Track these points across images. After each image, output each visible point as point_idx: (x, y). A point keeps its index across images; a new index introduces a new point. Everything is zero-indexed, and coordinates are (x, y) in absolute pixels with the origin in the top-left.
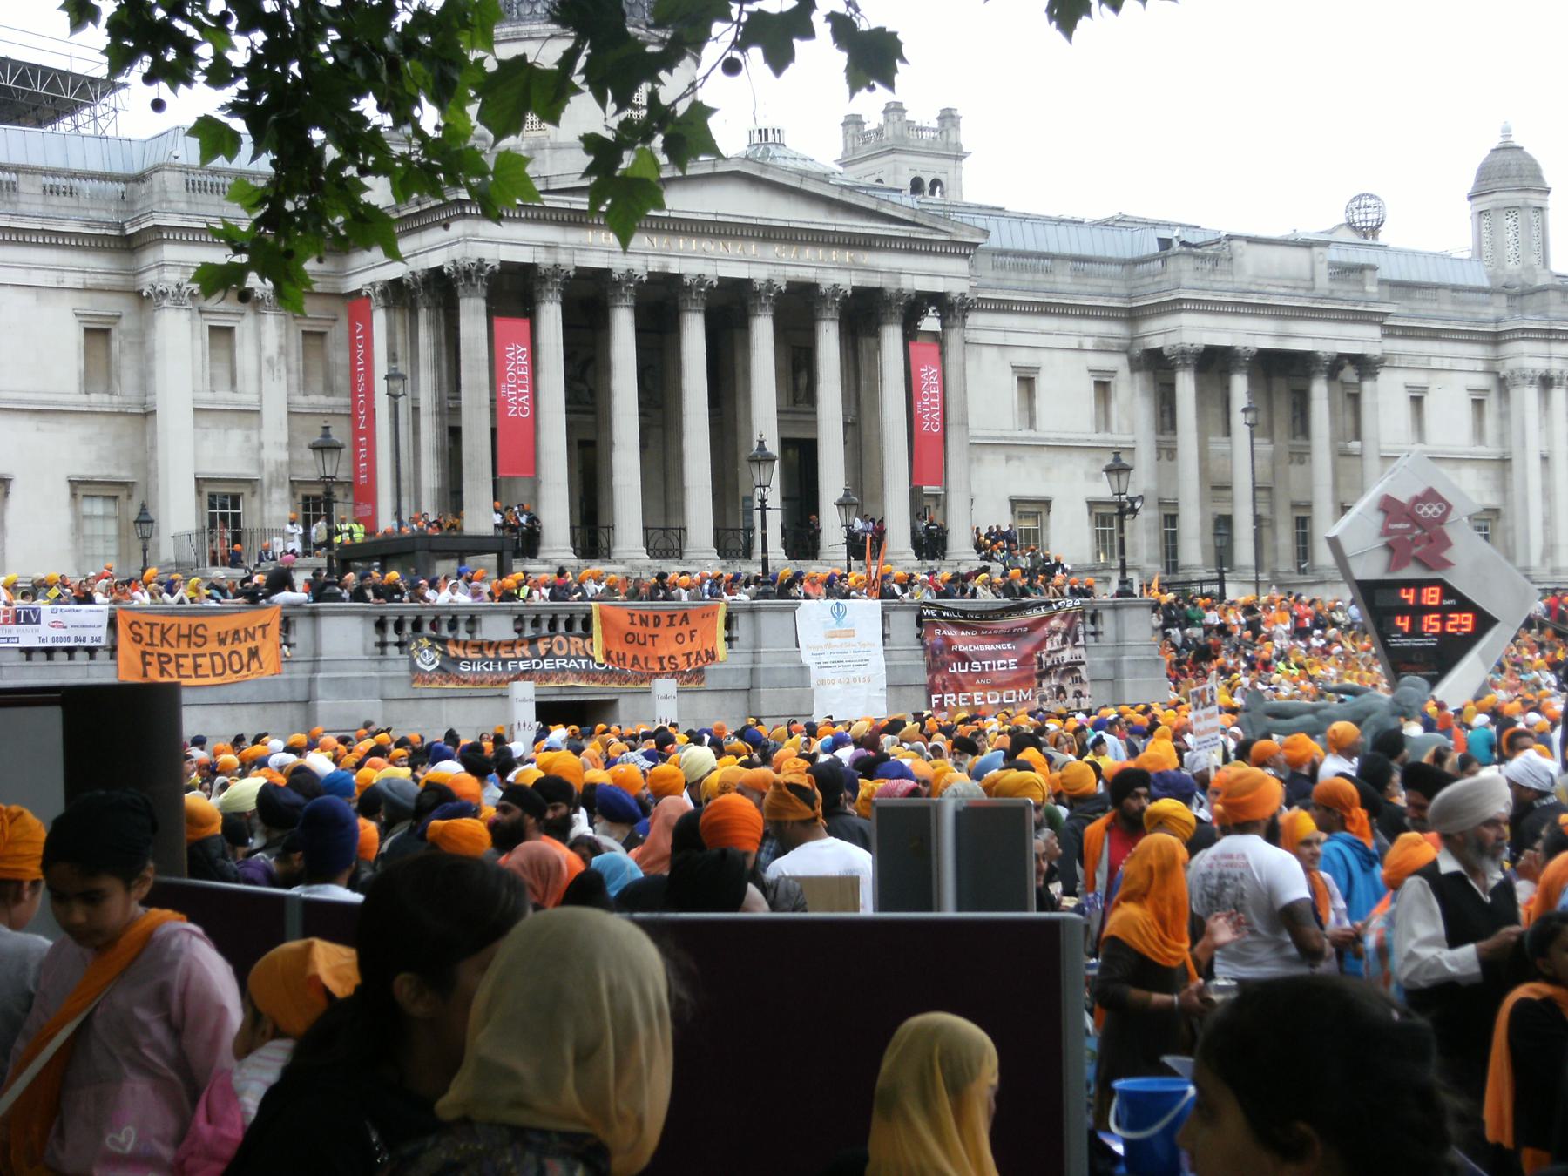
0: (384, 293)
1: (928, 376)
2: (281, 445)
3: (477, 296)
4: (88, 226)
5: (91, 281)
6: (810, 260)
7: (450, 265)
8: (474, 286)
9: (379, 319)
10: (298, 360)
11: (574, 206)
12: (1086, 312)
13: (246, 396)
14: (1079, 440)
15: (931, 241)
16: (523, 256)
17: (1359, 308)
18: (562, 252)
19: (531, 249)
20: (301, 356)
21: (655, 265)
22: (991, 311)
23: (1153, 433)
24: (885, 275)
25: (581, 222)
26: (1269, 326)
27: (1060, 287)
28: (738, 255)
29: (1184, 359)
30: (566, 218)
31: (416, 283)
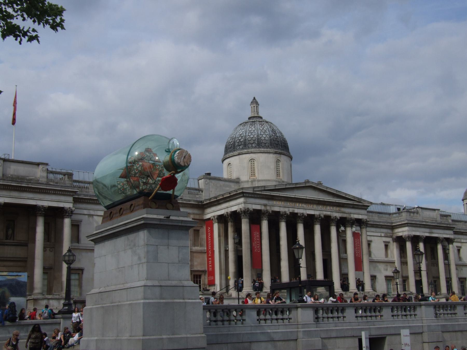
0: (217, 219)
7: (239, 210)
9: (216, 226)
10: (192, 237)
16: (258, 207)
17: (448, 226)
18: (268, 206)
19: (260, 206)
20: (193, 236)
21: (291, 210)
26: (428, 230)
27: (376, 220)
28: (311, 208)
29: (408, 238)
31: (228, 215)
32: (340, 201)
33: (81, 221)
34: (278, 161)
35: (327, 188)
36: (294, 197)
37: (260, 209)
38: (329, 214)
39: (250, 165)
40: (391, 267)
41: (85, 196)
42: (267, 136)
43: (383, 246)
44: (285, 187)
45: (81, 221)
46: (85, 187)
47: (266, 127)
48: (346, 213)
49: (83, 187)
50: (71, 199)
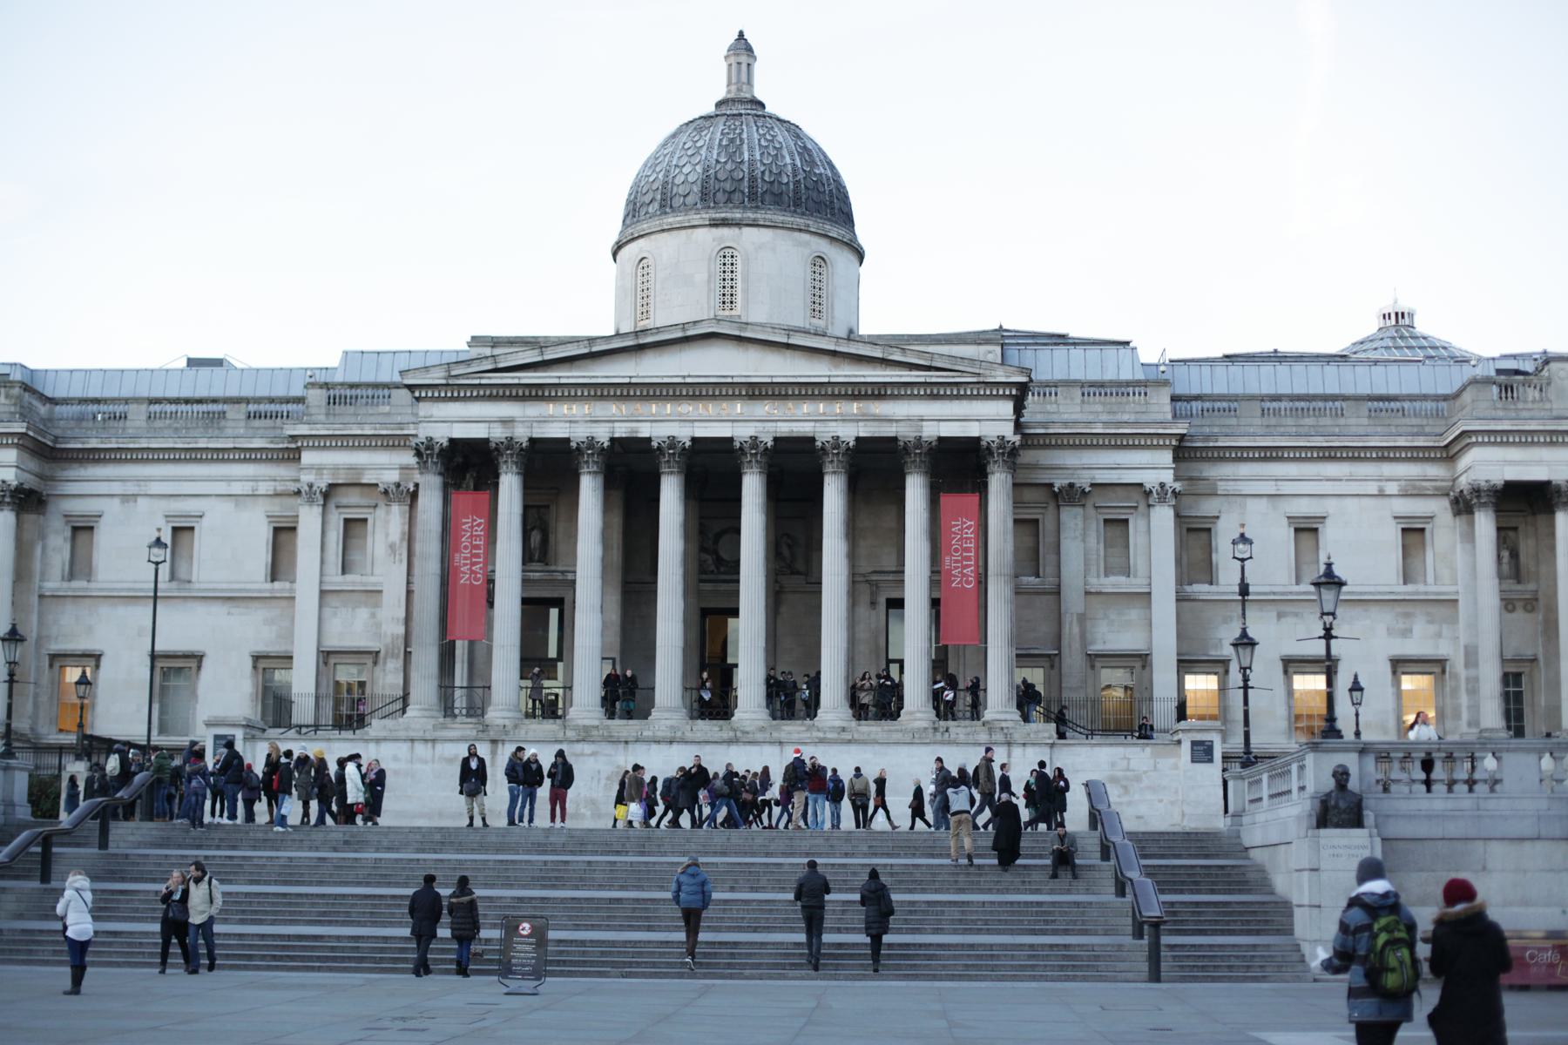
1: (961, 530)
2: (398, 620)
3: (428, 472)
4: (272, 442)
5: (280, 487)
6: (809, 414)
8: (426, 462)
12: (1385, 455)
13: (370, 581)
14: (1380, 593)
18: (520, 425)
19: (487, 425)
21: (621, 431)
22: (1253, 460)
24: (902, 424)
25: (537, 395)
27: (1354, 430)
29: (1478, 497)
32: (856, 376)
33: (100, 516)
34: (730, 250)
35: (790, 331)
36: (627, 380)
37: (485, 436)
38: (807, 429)
40: (1431, 622)
41: (102, 443)
43: (1393, 535)
44: (586, 351)
45: (100, 516)
46: (118, 415)
47: (707, 138)
50: (11, 455)
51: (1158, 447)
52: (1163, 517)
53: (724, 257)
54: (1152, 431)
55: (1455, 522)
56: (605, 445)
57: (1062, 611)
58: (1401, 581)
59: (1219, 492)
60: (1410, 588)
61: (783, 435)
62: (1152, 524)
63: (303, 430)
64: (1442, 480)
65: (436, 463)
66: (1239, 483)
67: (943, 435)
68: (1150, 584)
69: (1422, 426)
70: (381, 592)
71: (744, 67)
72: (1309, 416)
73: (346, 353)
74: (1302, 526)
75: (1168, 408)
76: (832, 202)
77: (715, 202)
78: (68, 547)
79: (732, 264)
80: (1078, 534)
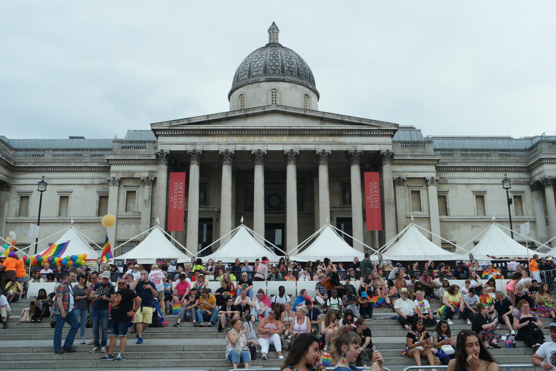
1: (373, 186)
4: (100, 164)
5: (102, 181)
6: (313, 142)
11: (200, 128)
12: (506, 170)
15: (370, 130)
16: (182, 148)
18: (199, 145)
19: (185, 145)
21: (239, 148)
22: (460, 171)
23: (544, 214)
25: (205, 134)
27: (494, 161)
29: (547, 182)
30: (199, 133)
33: (32, 192)
34: (275, 90)
36: (241, 128)
37: (185, 150)
39: (240, 103)
42: (262, 62)
45: (32, 192)
47: (265, 53)
48: (347, 144)
49: (37, 156)
51: (430, 164)
52: (433, 190)
53: (273, 92)
54: (428, 158)
55: (532, 193)
56: (233, 153)
57: (398, 224)
58: (515, 214)
59: (448, 183)
60: (518, 217)
61: (303, 149)
62: (429, 192)
63: (112, 157)
64: (526, 179)
65: (165, 160)
66: (455, 179)
67: (365, 150)
68: (429, 214)
69: (518, 160)
70: (141, 218)
71: (275, 33)
72: (478, 156)
73: (129, 131)
74: (478, 195)
75: (433, 151)
76: (310, 77)
77: (269, 73)
78: (19, 203)
79: (276, 95)
80: (402, 195)
